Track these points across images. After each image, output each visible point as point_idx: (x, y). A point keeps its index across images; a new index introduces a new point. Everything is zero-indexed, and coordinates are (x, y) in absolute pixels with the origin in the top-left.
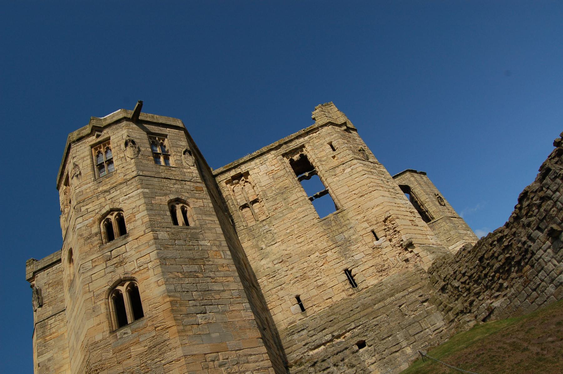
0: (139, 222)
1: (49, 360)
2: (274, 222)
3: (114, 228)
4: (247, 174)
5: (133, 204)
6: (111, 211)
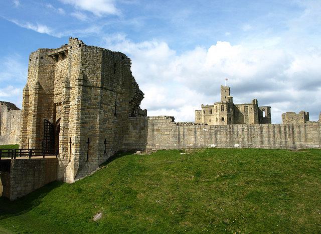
3: (223, 119)
5: (226, 117)
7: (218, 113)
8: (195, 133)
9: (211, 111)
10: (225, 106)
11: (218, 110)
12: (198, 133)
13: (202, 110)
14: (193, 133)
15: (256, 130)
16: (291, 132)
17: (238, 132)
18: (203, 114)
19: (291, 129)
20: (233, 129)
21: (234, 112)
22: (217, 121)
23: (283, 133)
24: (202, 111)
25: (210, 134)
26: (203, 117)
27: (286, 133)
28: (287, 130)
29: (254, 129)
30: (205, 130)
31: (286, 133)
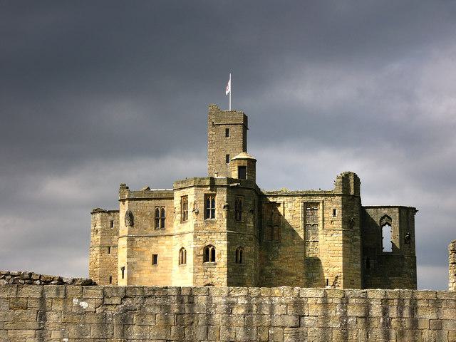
0: (222, 260)
1: (134, 263)
2: (282, 247)
3: (208, 255)
4: (279, 204)
5: (221, 247)
6: (210, 246)
7: (190, 226)
8: (42, 316)
9: (159, 219)
10: (221, 198)
11: (191, 215)
12: (52, 317)
13: (124, 209)
14: (31, 316)
15: (279, 310)
16: (407, 324)
17: (209, 316)
18: (123, 228)
19: (406, 313)
20: (191, 303)
21: (260, 226)
22: (183, 261)
23: (377, 323)
24: (122, 215)
25: (103, 323)
26: (123, 243)
27: (387, 324)
28: (393, 312)
29: (272, 307)
30: (84, 305)
31: (387, 324)
